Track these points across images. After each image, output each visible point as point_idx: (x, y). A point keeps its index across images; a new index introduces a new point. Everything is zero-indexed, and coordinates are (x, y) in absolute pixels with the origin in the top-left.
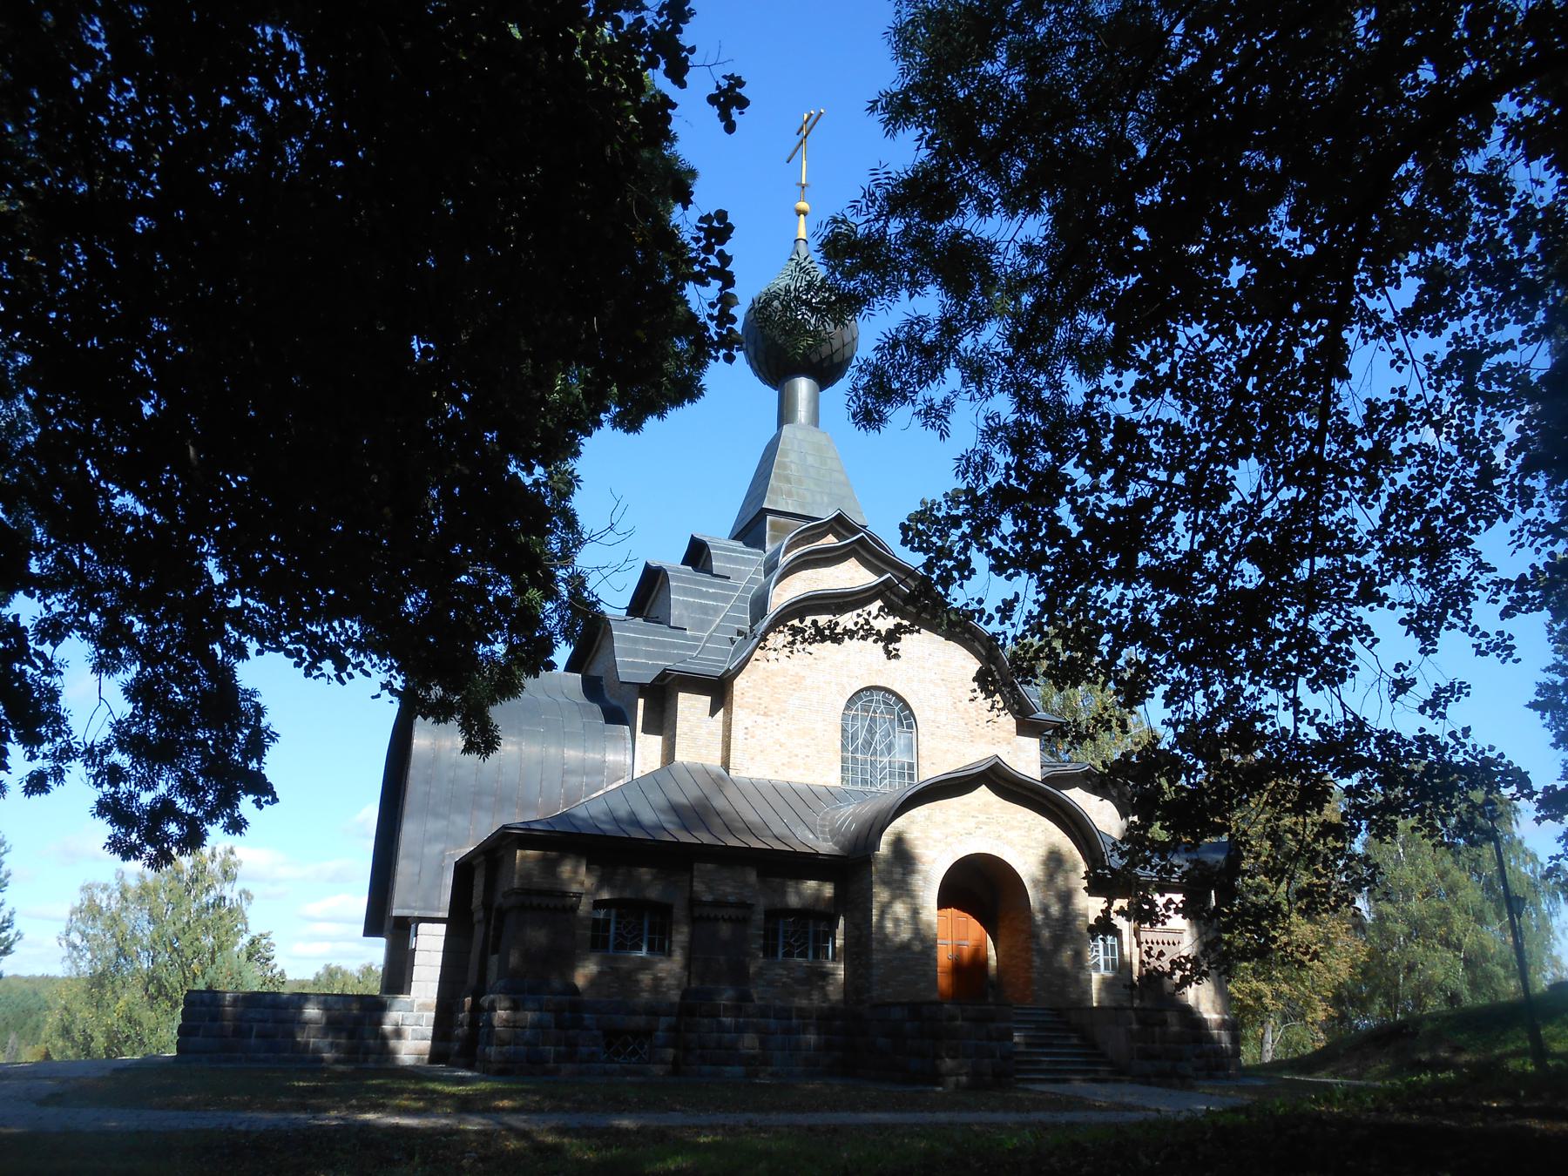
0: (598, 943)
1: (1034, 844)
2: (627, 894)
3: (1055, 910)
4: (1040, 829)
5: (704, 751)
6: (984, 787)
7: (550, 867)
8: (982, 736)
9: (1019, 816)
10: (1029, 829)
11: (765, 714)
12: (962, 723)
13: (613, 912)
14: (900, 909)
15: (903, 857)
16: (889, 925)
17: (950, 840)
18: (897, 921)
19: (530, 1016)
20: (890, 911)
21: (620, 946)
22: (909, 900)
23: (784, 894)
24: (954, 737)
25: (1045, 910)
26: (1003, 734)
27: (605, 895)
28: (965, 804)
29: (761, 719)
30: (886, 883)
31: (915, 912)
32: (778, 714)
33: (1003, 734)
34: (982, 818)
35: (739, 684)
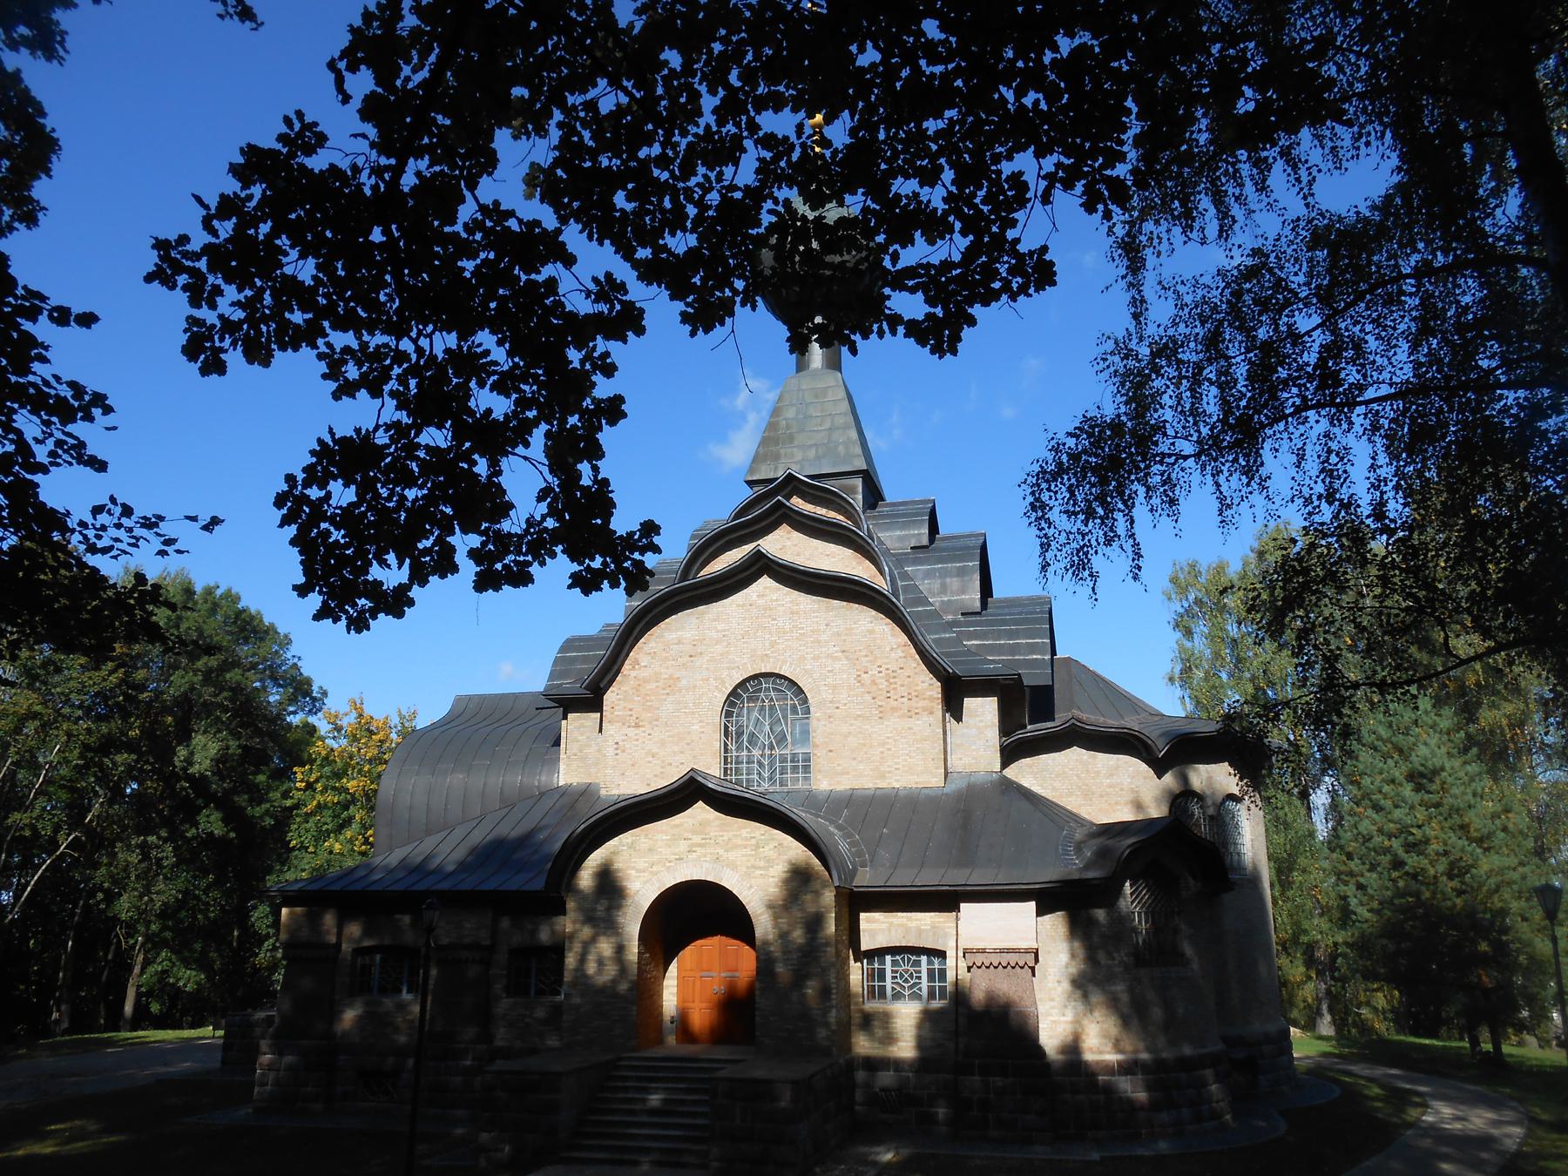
0: (360, 986)
1: (762, 864)
2: (387, 941)
3: (798, 935)
4: (771, 846)
5: (593, 770)
6: (700, 803)
7: (314, 919)
8: (894, 709)
9: (744, 833)
10: (757, 846)
11: (637, 726)
12: (868, 698)
13: (378, 957)
14: (605, 947)
15: (610, 887)
16: (591, 968)
17: (655, 869)
18: (601, 962)
19: (289, 1059)
20: (593, 950)
21: (383, 991)
22: (613, 940)
23: (534, 932)
24: (859, 716)
25: (783, 936)
26: (922, 703)
27: (367, 943)
28: (677, 826)
29: (632, 732)
30: (590, 918)
31: (620, 949)
32: (650, 723)
33: (922, 703)
34: (697, 839)
35: (610, 698)
